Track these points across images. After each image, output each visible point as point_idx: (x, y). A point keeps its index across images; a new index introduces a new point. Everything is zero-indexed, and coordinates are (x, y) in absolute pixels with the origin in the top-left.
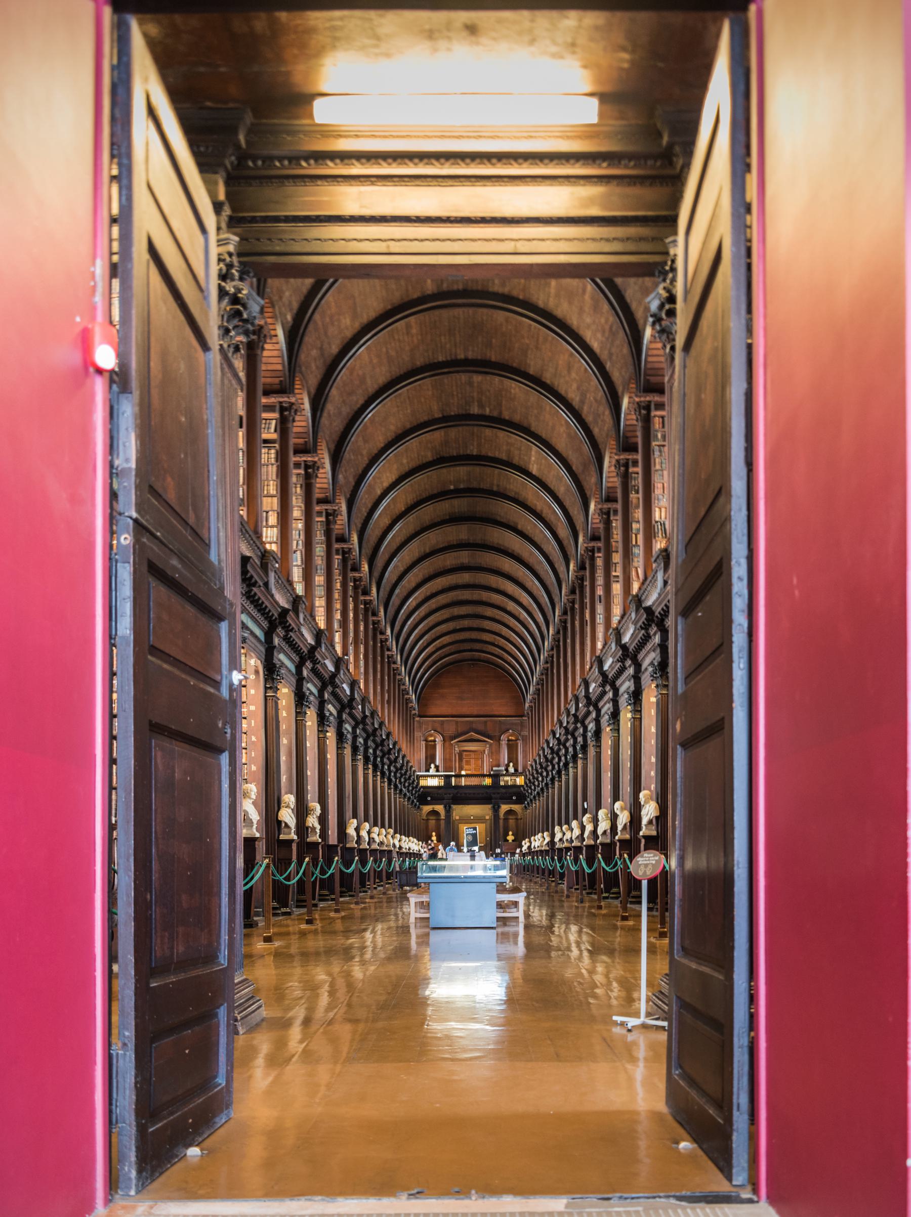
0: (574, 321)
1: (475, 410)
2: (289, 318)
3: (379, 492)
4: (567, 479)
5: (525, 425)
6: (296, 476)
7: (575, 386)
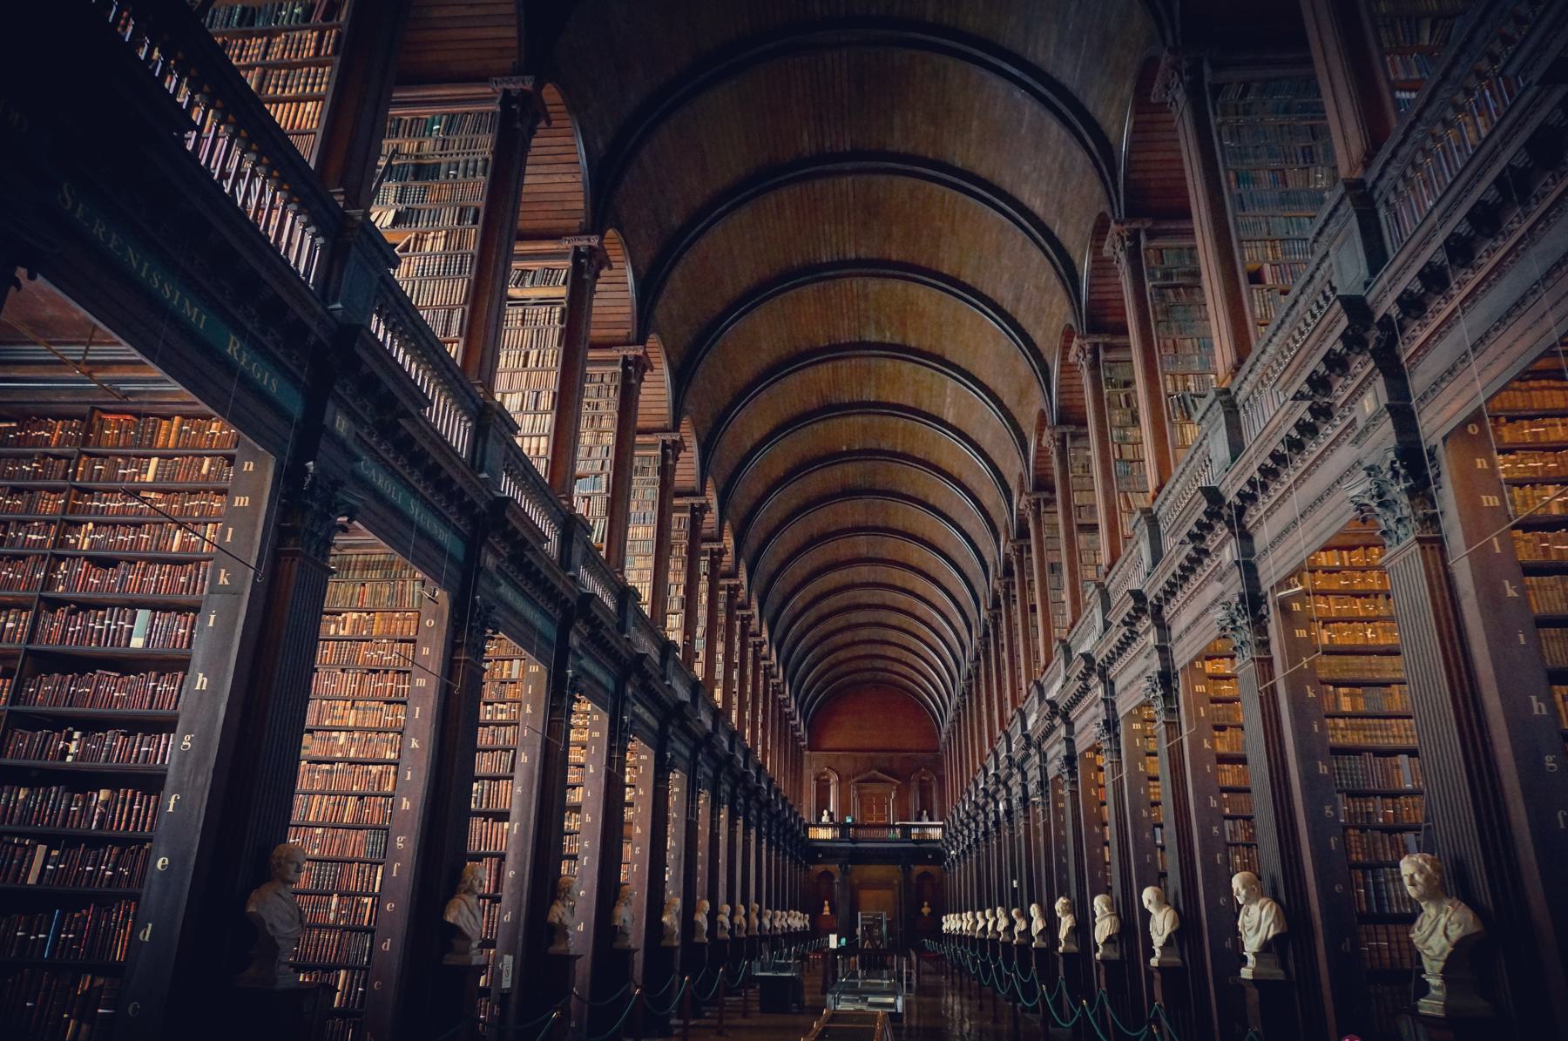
5: (939, 352)
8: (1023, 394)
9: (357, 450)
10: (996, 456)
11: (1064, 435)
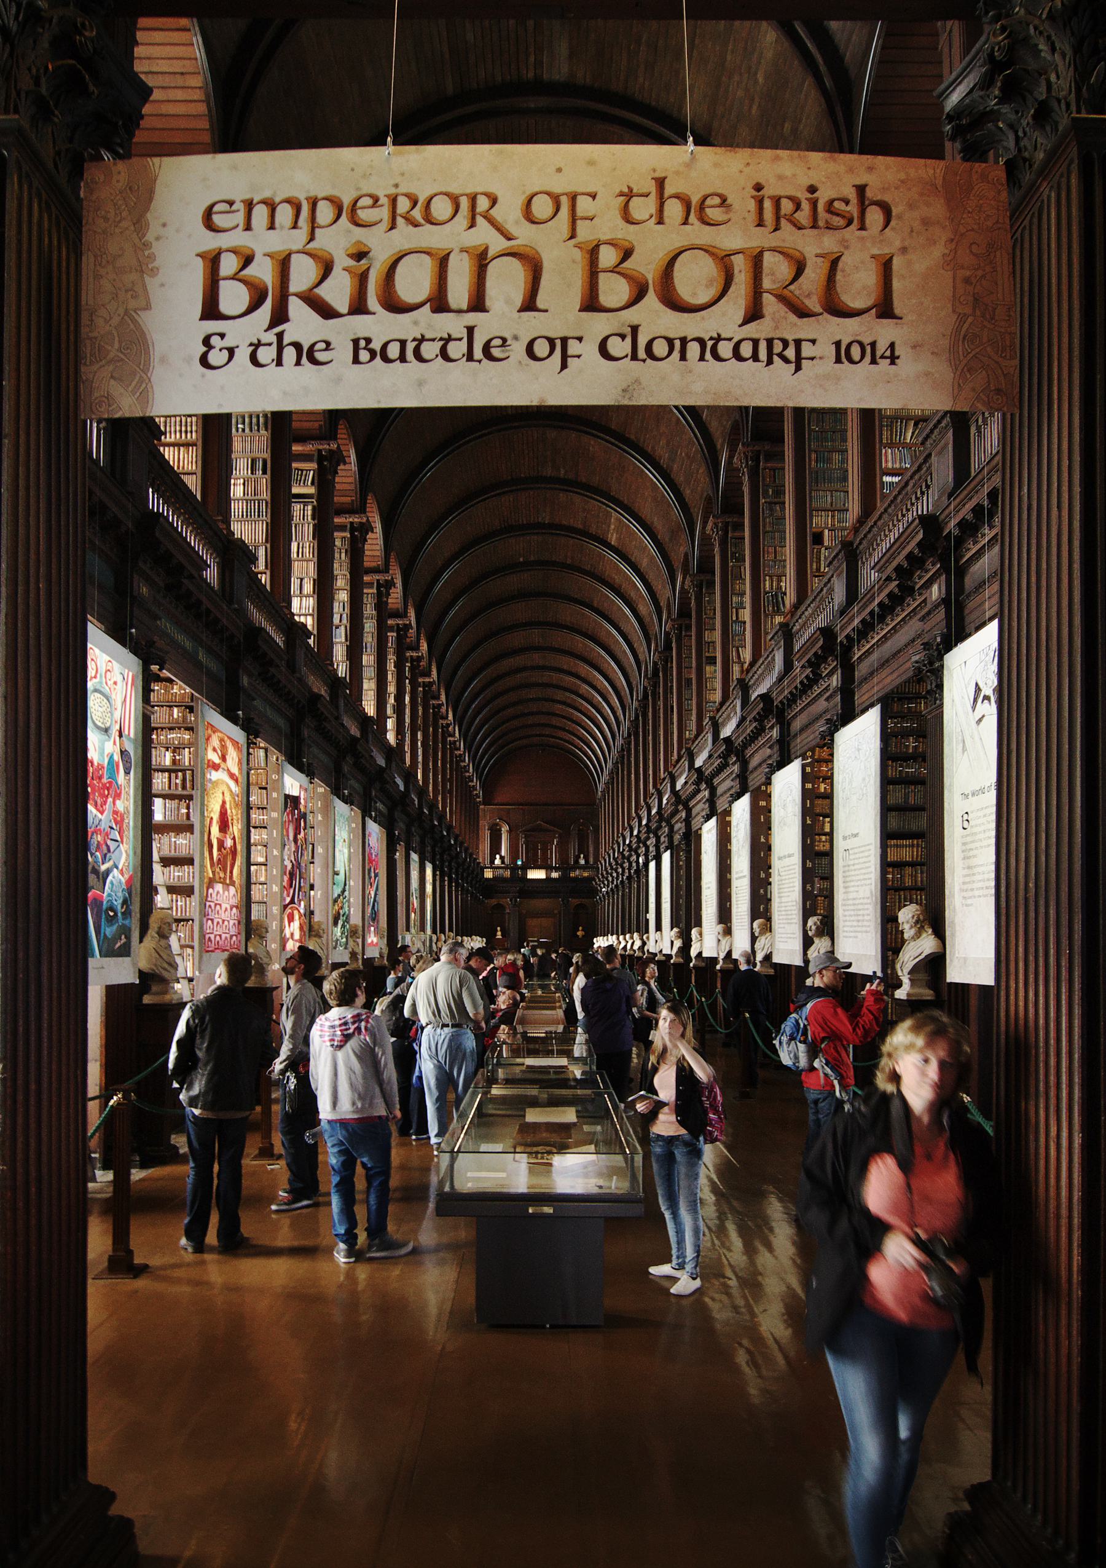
6: (340, 540)
8: (674, 533)
9: (254, 694)
10: (651, 577)
11: (702, 581)
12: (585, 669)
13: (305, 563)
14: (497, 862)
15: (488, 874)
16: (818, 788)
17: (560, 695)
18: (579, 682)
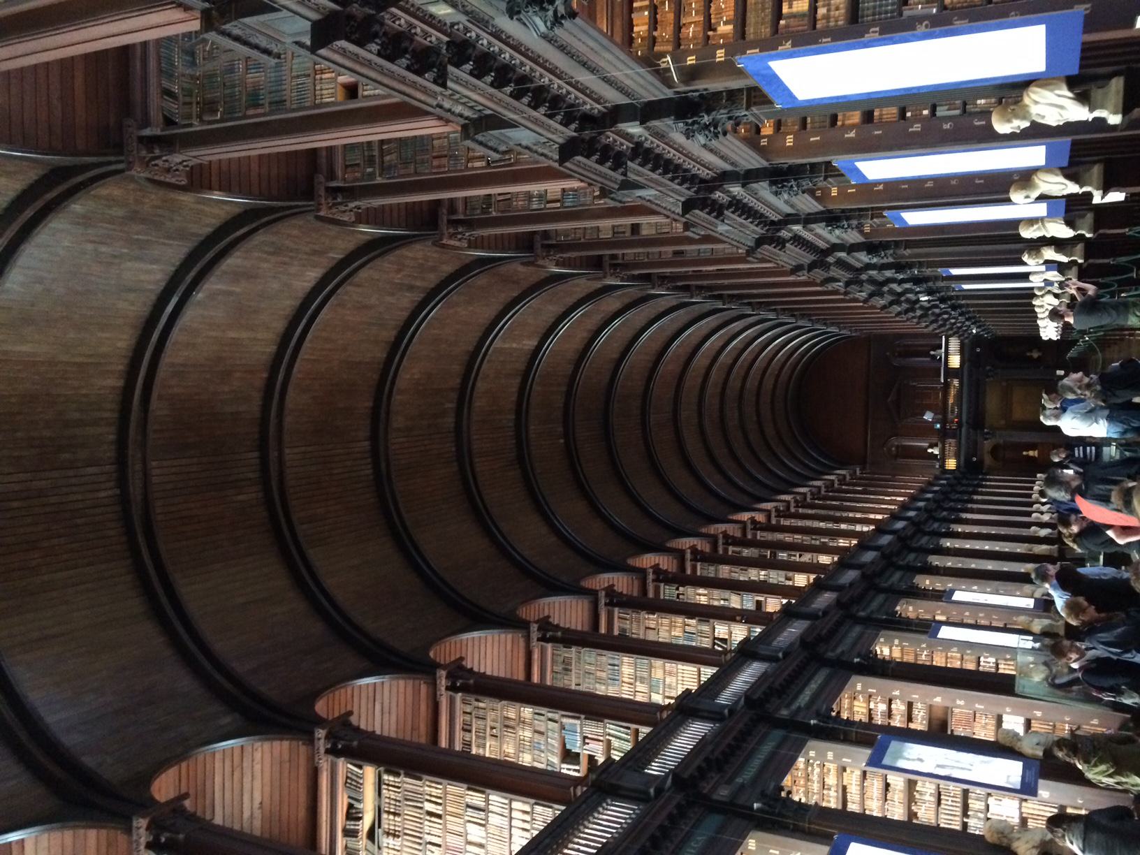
0: (288, 304)
1: (450, 420)
2: (226, 720)
3: (554, 539)
4: (534, 303)
7: (389, 299)
12: (701, 360)
13: (449, 797)
14: (936, 451)
15: (951, 464)
16: (723, 36)
17: (734, 382)
18: (717, 364)
